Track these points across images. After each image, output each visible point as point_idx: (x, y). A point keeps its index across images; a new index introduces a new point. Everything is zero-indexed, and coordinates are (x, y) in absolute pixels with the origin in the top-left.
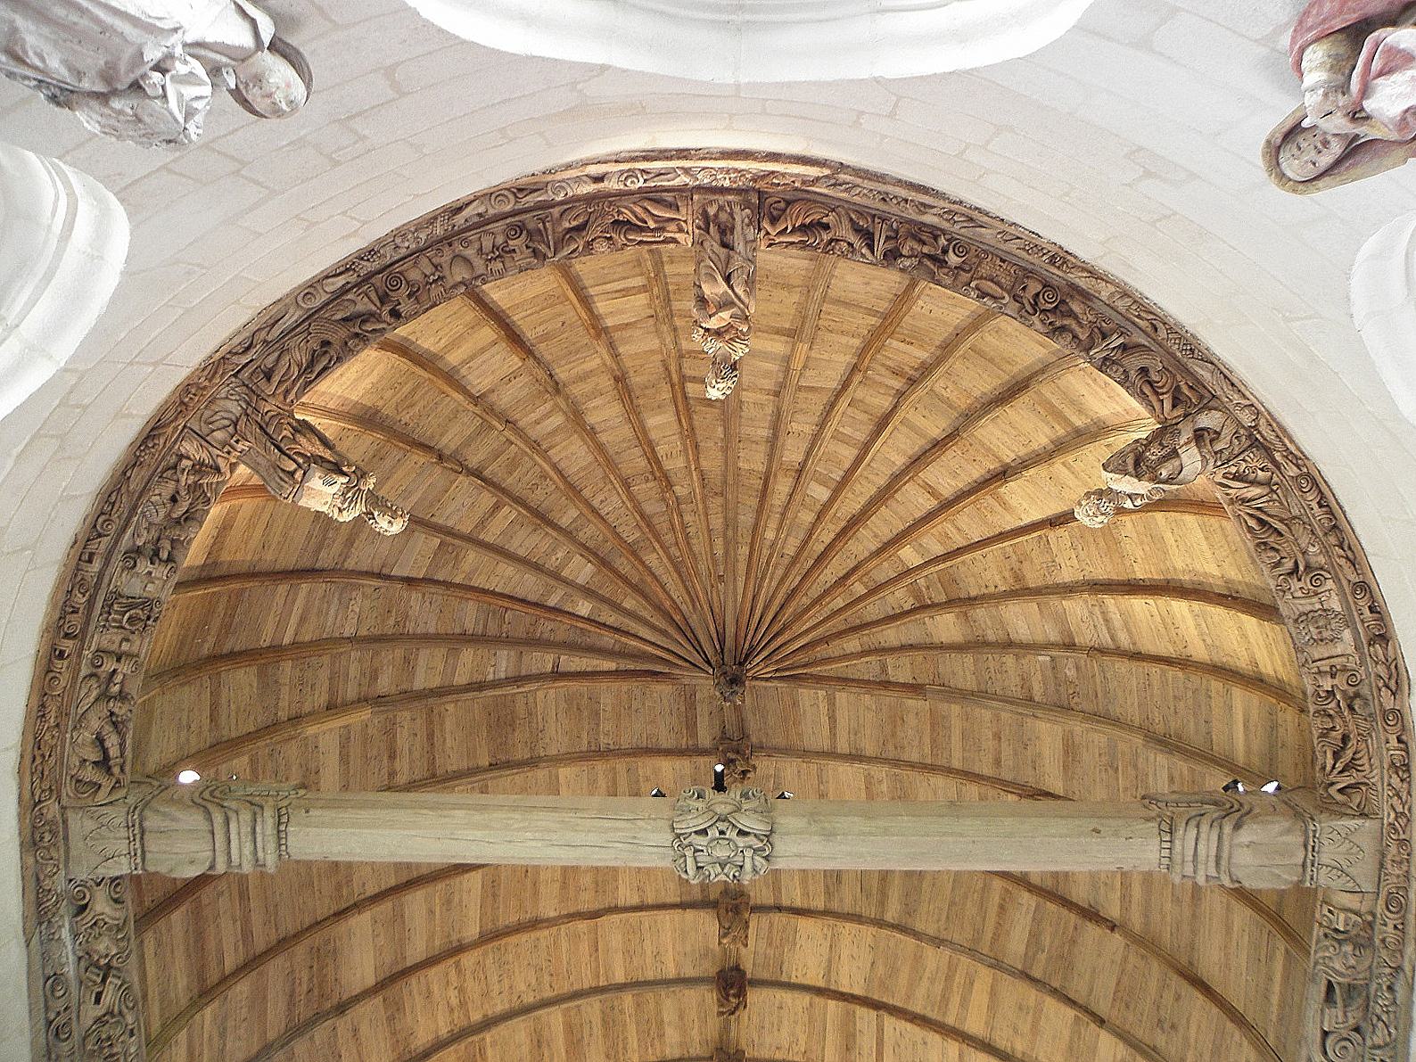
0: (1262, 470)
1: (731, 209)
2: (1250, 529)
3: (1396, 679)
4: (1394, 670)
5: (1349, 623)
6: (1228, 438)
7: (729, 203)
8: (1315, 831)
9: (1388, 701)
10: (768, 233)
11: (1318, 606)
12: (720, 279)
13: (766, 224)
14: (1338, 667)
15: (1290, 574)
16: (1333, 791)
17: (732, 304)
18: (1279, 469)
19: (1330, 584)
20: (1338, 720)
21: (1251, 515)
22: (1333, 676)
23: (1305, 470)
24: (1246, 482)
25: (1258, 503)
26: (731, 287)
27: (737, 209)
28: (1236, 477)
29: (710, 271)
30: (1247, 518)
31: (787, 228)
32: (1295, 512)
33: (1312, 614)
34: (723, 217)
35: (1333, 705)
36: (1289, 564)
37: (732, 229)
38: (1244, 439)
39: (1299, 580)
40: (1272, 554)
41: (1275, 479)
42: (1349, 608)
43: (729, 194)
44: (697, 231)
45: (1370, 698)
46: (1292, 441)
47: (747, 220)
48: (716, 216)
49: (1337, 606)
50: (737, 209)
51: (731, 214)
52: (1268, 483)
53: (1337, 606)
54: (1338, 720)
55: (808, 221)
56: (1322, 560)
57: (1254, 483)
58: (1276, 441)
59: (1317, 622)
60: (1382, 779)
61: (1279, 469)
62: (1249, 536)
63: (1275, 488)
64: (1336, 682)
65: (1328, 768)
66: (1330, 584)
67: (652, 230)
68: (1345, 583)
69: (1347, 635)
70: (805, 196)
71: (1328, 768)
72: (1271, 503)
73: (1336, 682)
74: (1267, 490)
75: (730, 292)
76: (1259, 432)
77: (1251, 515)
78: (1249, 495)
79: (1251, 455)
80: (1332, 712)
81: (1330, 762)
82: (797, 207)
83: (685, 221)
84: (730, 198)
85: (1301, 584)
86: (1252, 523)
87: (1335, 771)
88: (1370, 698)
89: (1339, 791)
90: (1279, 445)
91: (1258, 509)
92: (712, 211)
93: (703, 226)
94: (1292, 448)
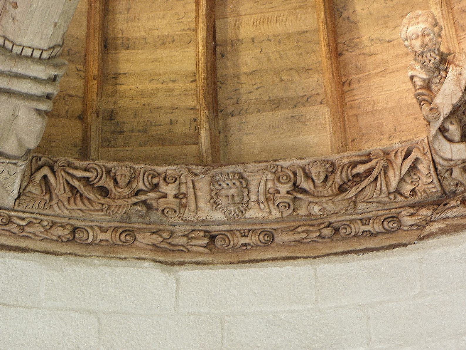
0: (413, 190)
2: (355, 165)
3: (169, 253)
4: (177, 248)
5: (229, 221)
6: (461, 179)
8: (15, 164)
9: (145, 239)
11: (253, 197)
14: (184, 201)
15: (294, 184)
16: (46, 171)
18: (412, 206)
19: (276, 214)
20: (126, 191)
21: (370, 171)
22: (176, 196)
23: (405, 228)
24: (406, 174)
25: (381, 181)
28: (413, 168)
30: (367, 166)
32: (362, 206)
33: (247, 192)
35: (141, 186)
36: (305, 185)
38: (453, 188)
39: (288, 192)
40: (322, 177)
41: (399, 198)
42: (247, 223)
45: (147, 220)
46: (443, 232)
49: (252, 213)
52: (398, 192)
53: (252, 213)
54: (126, 191)
56: (303, 212)
57: (402, 180)
58: (444, 215)
59: (238, 195)
60: (58, 216)
61: (412, 206)
62: (346, 161)
63: (392, 196)
64: (170, 198)
65: (71, 171)
66: (276, 214)
68: (275, 226)
69: (218, 216)
71: (71, 171)
72: (378, 192)
73: (170, 198)
74: (392, 189)
76: (457, 206)
77: (370, 171)
78: (391, 173)
79: (434, 190)
80: (134, 185)
81: (80, 174)
85: (283, 192)
86: (361, 169)
87: (69, 179)
88: (147, 220)
89: (45, 177)
90: (439, 216)
91: (376, 179)
94: (434, 227)
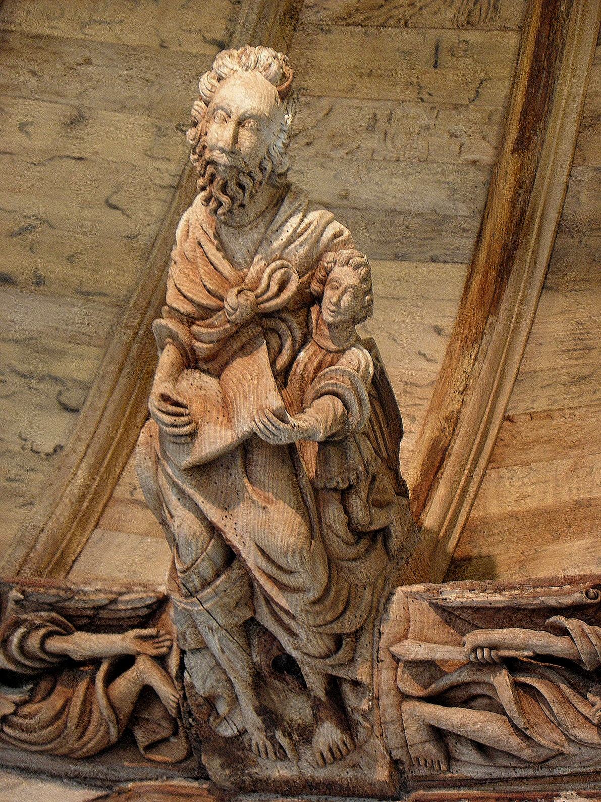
1: (272, 739)
7: (281, 754)
10: (161, 660)
12: (251, 557)
13: (167, 692)
17: (203, 470)
26: (213, 529)
27: (257, 737)
29: (284, 578)
31: (110, 679)
34: (297, 709)
37: (258, 683)
43: (287, 782)
44: (361, 674)
47: (222, 708)
48: (317, 720)
50: (257, 737)
51: (271, 719)
55: (56, 701)
67: (513, 665)
70: (84, 768)
75: (214, 514)
82: (93, 739)
83: (405, 697)
84: (281, 771)
92: (328, 734)
93: (347, 689)
